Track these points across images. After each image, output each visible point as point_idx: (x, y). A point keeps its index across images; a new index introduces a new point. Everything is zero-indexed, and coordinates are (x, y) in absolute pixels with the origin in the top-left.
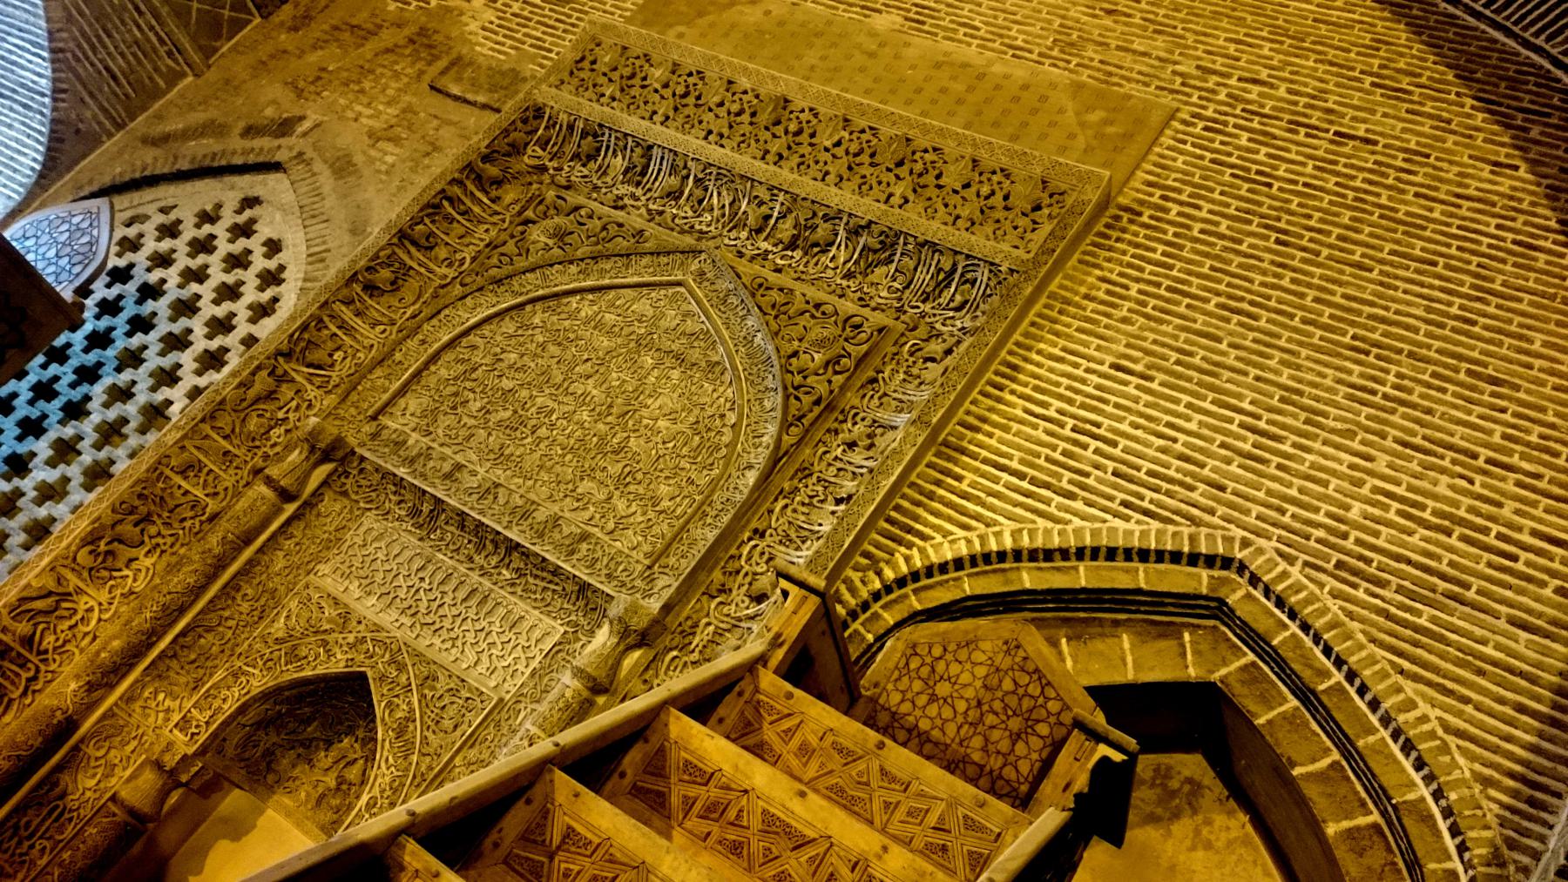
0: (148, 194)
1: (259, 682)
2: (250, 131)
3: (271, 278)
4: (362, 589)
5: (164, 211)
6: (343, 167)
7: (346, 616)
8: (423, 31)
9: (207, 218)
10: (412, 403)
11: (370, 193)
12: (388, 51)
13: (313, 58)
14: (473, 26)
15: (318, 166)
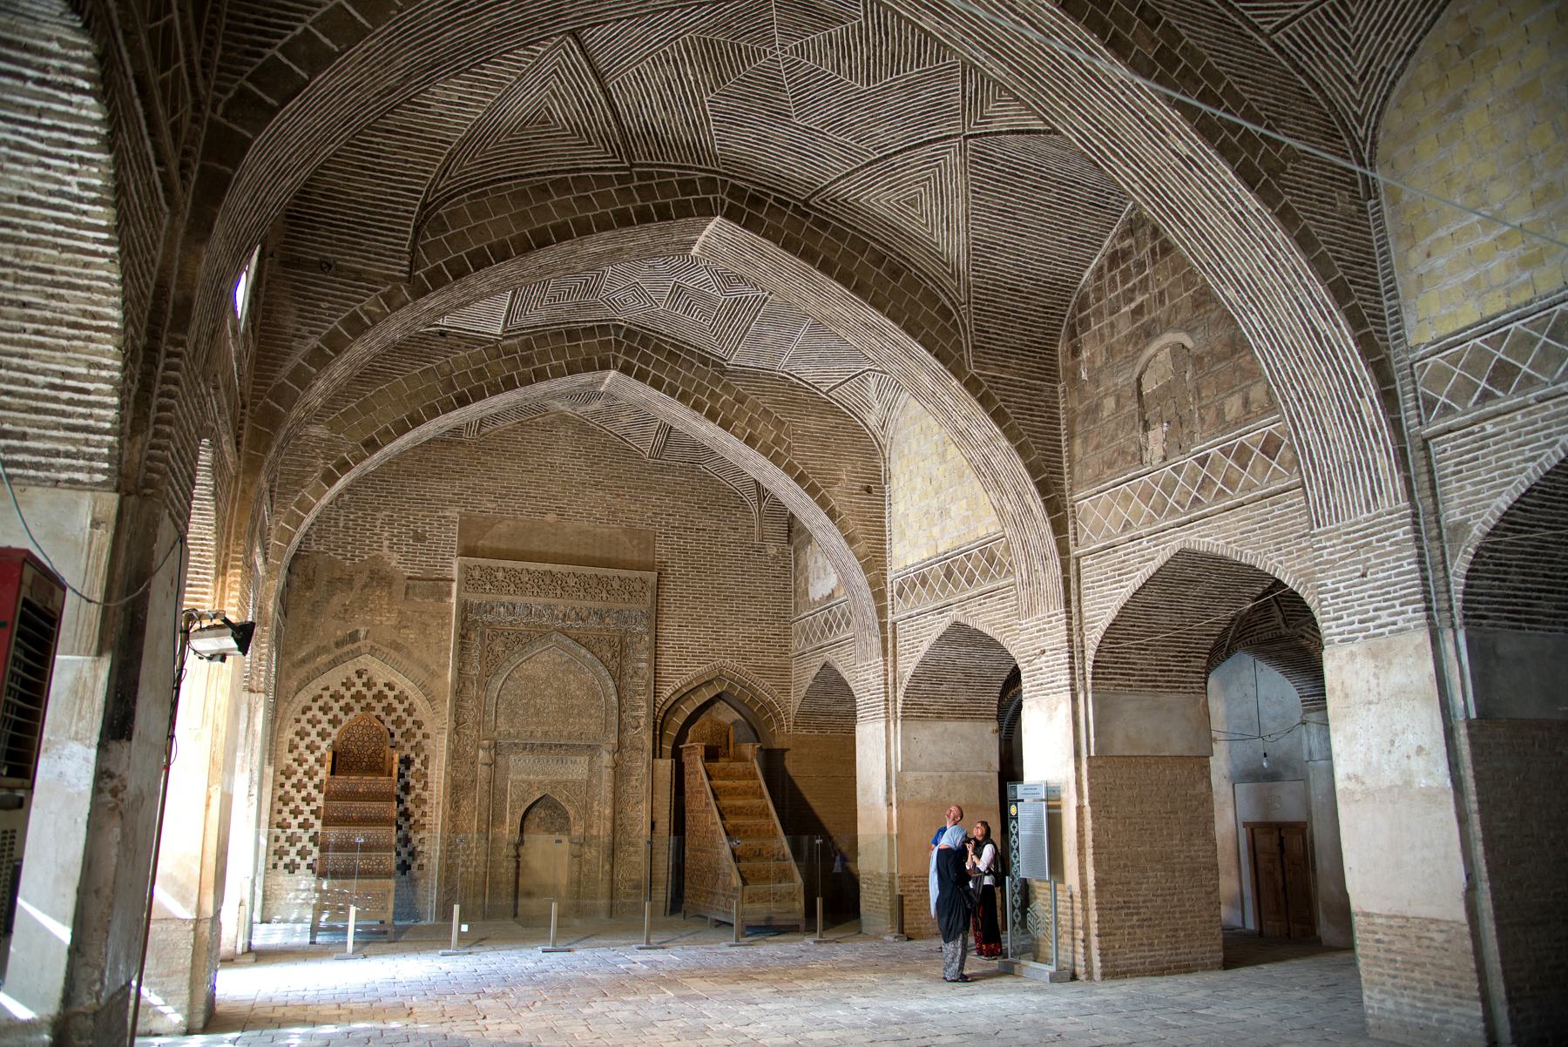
0: (312, 685)
1: (521, 812)
2: (338, 645)
3: (401, 698)
4: (525, 775)
5: (327, 689)
6: (396, 647)
7: (530, 784)
8: (372, 572)
9: (347, 685)
10: (501, 720)
11: (416, 654)
12: (365, 586)
13: (335, 600)
14: (394, 563)
15: (386, 650)
